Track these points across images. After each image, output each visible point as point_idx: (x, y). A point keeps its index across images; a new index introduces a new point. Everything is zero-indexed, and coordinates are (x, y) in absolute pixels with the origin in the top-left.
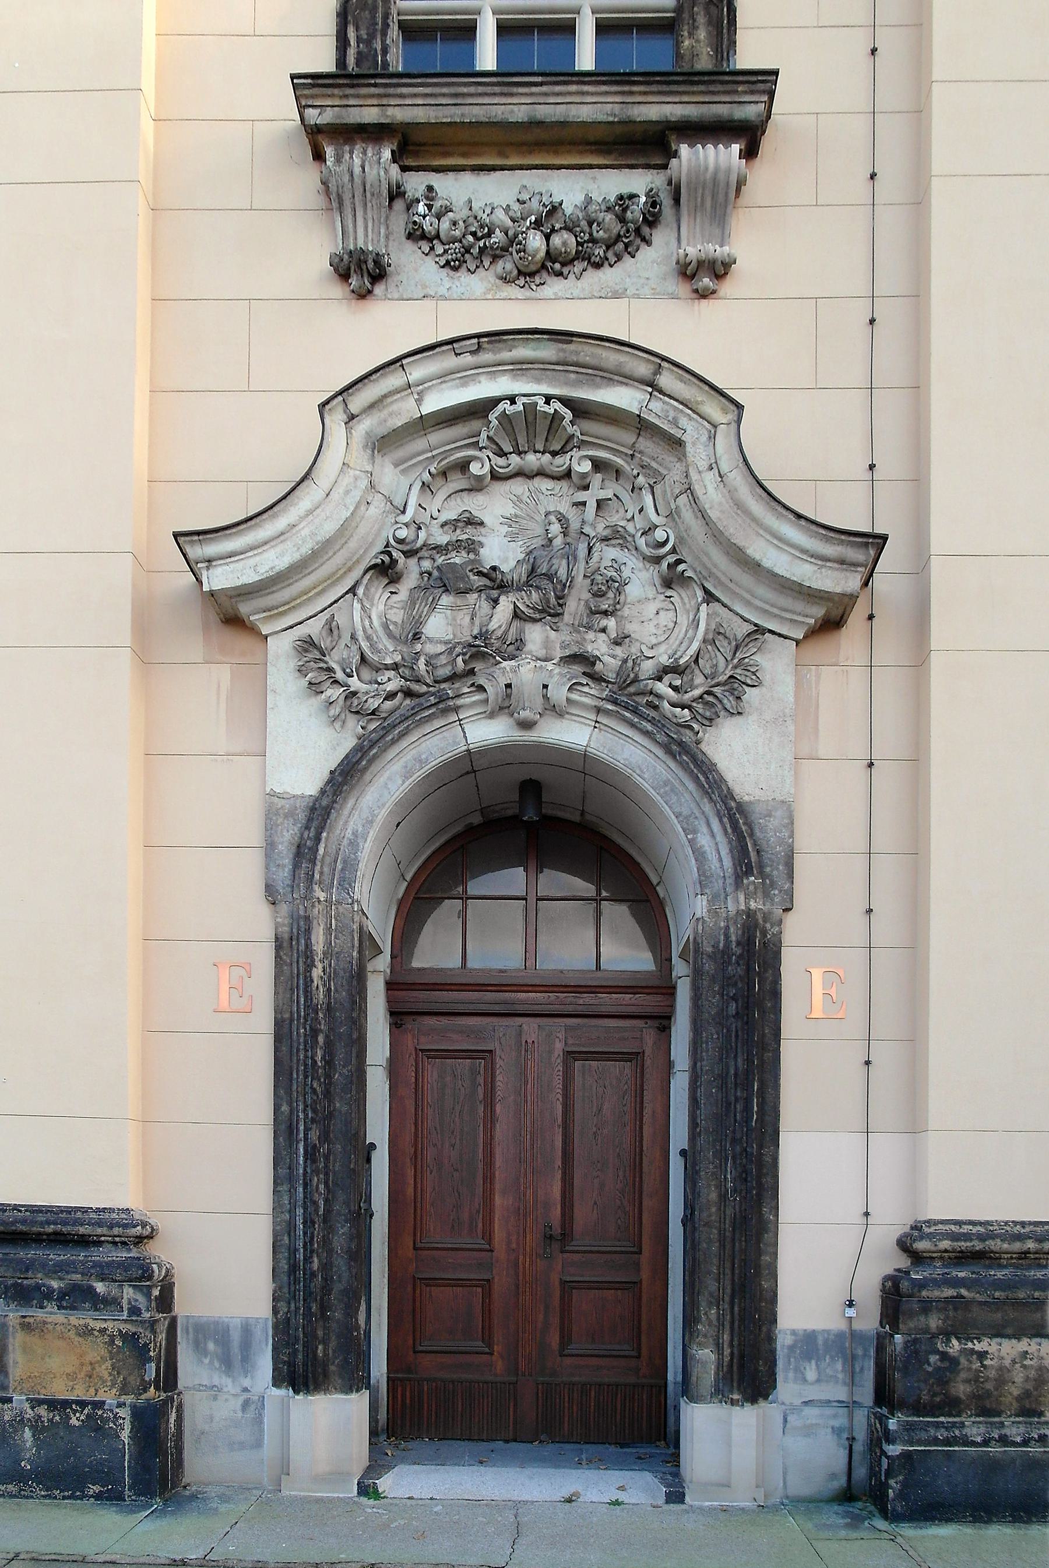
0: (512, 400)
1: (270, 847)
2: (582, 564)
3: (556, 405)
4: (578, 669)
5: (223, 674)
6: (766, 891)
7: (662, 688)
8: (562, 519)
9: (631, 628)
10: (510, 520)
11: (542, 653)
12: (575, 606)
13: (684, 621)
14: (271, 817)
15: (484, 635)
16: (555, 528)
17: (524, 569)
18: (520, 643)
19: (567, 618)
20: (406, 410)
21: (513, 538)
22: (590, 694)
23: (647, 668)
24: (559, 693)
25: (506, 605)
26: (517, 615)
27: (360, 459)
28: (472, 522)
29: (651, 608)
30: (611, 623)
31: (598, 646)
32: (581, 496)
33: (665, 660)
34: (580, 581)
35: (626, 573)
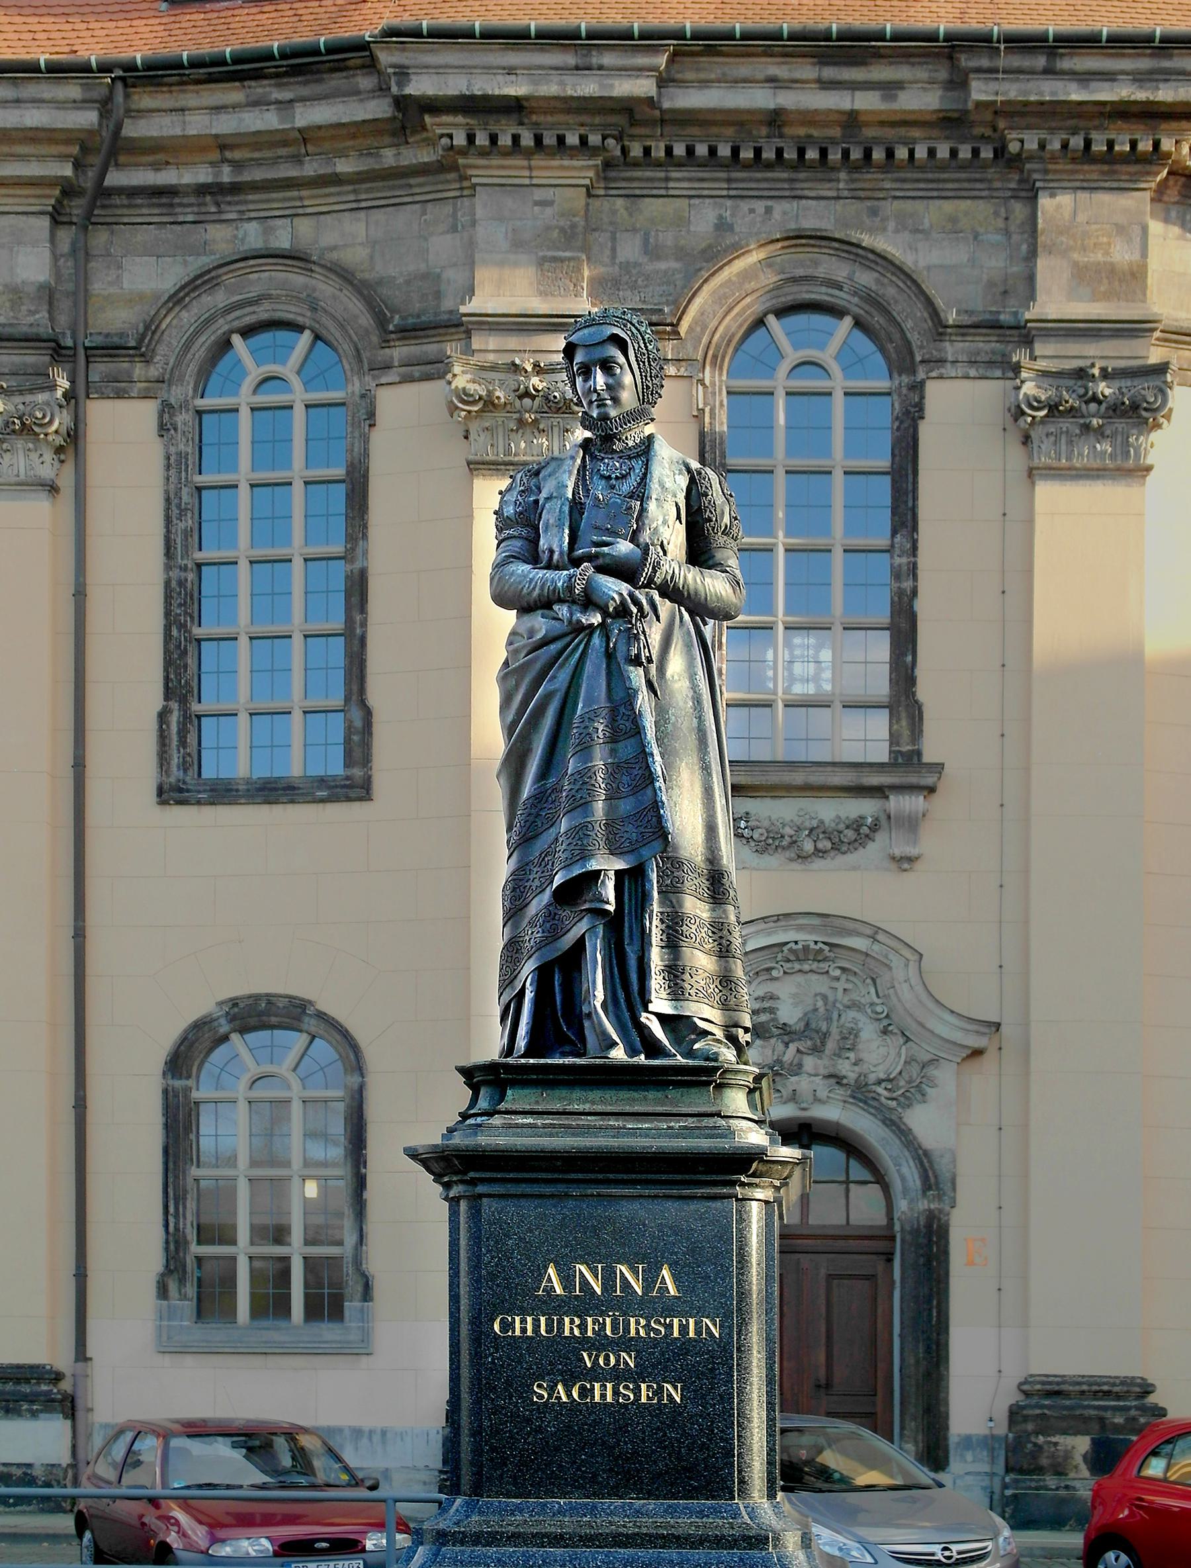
0: (796, 943)
2: (835, 1023)
3: (821, 945)
4: (833, 1081)
6: (940, 1198)
7: (880, 1090)
8: (825, 998)
9: (864, 1055)
10: (795, 996)
11: (813, 1072)
12: (831, 1045)
13: (893, 1052)
16: (820, 1004)
17: (802, 1025)
18: (800, 1066)
19: (827, 1052)
21: (796, 1005)
22: (840, 1092)
23: (872, 1078)
24: (822, 1093)
25: (792, 1047)
26: (798, 1051)
28: (772, 997)
29: (874, 1045)
30: (852, 1055)
31: (845, 1068)
32: (835, 984)
33: (882, 1076)
34: (834, 1030)
35: (861, 1025)
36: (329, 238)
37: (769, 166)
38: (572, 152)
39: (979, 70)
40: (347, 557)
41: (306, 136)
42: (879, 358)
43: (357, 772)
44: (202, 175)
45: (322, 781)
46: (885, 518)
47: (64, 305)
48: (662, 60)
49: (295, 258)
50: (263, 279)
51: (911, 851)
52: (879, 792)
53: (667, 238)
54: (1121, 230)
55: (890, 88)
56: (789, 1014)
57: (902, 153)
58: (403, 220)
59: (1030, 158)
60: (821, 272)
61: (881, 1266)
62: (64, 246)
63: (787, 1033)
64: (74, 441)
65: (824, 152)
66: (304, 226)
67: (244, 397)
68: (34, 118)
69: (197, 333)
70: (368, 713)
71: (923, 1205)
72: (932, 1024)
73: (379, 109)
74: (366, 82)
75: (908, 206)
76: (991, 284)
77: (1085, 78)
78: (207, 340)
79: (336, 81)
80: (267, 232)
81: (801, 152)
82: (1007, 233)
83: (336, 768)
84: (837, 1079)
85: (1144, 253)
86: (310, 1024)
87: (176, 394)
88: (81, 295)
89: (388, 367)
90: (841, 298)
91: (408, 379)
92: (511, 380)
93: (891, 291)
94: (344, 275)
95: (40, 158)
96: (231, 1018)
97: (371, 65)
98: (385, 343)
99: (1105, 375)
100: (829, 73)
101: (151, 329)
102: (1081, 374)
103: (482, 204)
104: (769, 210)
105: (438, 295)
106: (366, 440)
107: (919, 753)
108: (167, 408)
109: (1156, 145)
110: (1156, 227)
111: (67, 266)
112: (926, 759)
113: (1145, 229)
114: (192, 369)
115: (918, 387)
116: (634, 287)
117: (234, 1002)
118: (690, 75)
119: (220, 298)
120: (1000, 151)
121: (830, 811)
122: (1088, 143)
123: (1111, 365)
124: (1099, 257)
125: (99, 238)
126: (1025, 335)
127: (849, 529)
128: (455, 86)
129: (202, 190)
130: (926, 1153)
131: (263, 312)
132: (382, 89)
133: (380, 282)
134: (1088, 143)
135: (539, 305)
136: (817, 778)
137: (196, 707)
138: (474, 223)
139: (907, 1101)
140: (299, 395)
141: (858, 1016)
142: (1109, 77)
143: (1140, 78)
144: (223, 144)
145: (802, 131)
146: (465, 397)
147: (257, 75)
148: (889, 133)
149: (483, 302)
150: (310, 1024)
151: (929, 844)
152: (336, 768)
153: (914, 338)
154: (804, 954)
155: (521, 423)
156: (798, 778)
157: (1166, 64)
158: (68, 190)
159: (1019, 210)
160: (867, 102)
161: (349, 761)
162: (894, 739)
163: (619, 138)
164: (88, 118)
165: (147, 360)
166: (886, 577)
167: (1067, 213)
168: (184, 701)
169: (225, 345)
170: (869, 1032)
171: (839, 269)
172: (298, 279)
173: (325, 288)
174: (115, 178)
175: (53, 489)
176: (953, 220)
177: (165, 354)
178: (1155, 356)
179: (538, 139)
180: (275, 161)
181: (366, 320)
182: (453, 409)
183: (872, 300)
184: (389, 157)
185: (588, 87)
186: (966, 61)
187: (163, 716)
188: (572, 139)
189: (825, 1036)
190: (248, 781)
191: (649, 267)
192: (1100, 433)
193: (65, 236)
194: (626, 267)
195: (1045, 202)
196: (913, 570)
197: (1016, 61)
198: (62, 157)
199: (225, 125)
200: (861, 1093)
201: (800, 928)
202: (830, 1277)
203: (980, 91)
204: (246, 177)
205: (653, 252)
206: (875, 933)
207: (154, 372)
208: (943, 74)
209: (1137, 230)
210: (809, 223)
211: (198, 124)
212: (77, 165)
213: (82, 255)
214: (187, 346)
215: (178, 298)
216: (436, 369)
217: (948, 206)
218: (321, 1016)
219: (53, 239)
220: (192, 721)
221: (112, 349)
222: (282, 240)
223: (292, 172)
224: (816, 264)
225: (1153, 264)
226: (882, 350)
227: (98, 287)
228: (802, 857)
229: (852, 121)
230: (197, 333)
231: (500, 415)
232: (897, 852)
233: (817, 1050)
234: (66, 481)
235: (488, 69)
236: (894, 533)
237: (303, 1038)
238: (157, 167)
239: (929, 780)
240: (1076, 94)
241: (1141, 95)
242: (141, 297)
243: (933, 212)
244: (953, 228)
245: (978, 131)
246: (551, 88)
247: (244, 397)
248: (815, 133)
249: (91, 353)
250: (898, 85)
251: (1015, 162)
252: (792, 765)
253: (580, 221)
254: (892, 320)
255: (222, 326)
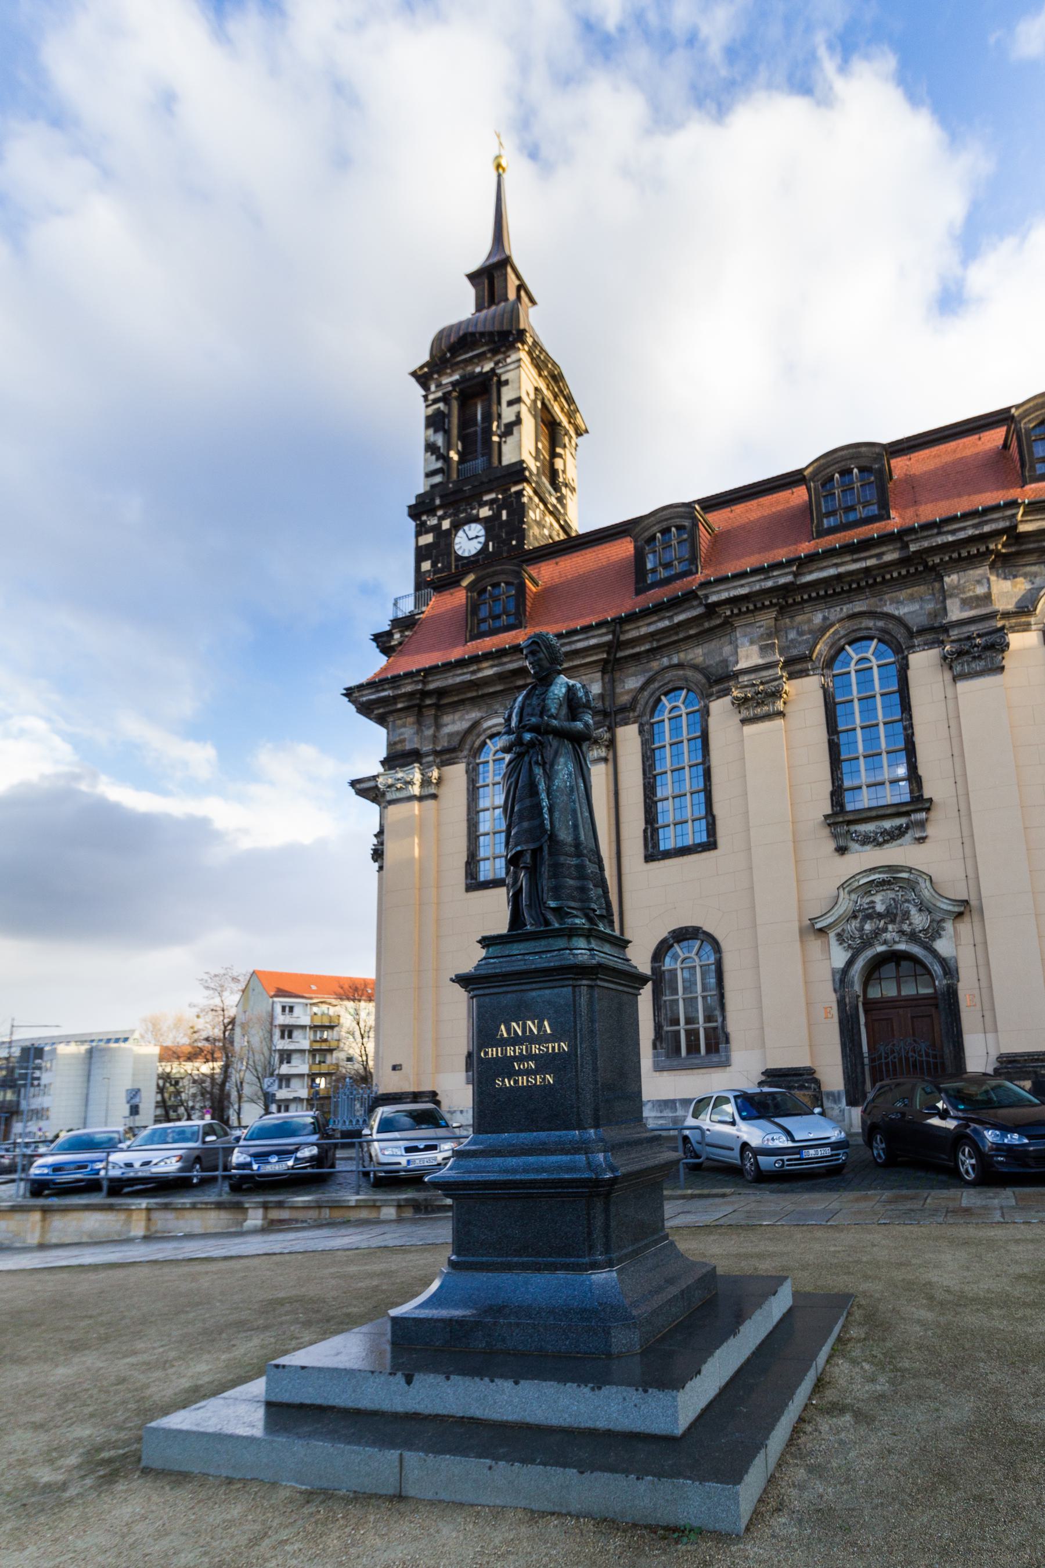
1: (834, 980)
5: (819, 942)
6: (952, 978)
12: (898, 919)
14: (834, 972)
15: (878, 928)
20: (856, 884)
22: (904, 938)
24: (897, 939)
25: (882, 922)
27: (847, 896)
28: (873, 902)
31: (905, 927)
36: (690, 656)
37: (839, 594)
38: (768, 607)
39: (912, 540)
40: (703, 763)
41: (680, 624)
42: (889, 651)
43: (712, 839)
44: (647, 647)
45: (700, 845)
46: (898, 709)
47: (607, 698)
48: (794, 568)
49: (680, 666)
50: (669, 675)
51: (924, 835)
52: (907, 814)
53: (806, 628)
54: (979, 582)
55: (879, 556)
56: (880, 908)
57: (888, 577)
58: (713, 645)
59: (938, 565)
60: (863, 625)
61: (933, 1009)
62: (607, 680)
63: (880, 916)
64: (612, 744)
65: (858, 584)
66: (682, 655)
67: (666, 715)
68: (593, 642)
69: (650, 697)
70: (714, 817)
71: (945, 982)
72: (939, 904)
73: (700, 610)
74: (695, 603)
75: (894, 594)
76: (930, 614)
77: (953, 532)
78: (652, 700)
79: (686, 605)
80: (670, 659)
81: (850, 586)
82: (934, 594)
83: (704, 839)
84: (902, 932)
85: (989, 588)
86: (701, 936)
87: (645, 719)
88: (613, 695)
89: (711, 695)
90: (873, 633)
91: (719, 697)
92: (753, 689)
93: (891, 626)
94: (695, 667)
95: (596, 654)
96: (673, 937)
97: (697, 597)
98: (711, 687)
99: (979, 636)
100: (855, 556)
101: (634, 701)
102: (969, 638)
103: (738, 634)
104: (841, 609)
105: (727, 667)
106: (707, 721)
107: (922, 796)
108: (641, 726)
109: (987, 548)
110: (993, 578)
111: (608, 686)
112: (926, 796)
113: (988, 580)
114: (648, 710)
115: (906, 658)
116: (795, 647)
117: (674, 931)
118: (805, 570)
119: (656, 685)
120: (926, 566)
121: (887, 824)
122: (959, 554)
123: (981, 632)
124: (971, 594)
125: (617, 675)
126: (945, 629)
127: (884, 716)
128: (724, 595)
129: (648, 651)
130: (944, 959)
131: (670, 686)
132: (701, 603)
133: (708, 667)
134: (959, 554)
135: (760, 661)
136: (881, 812)
137: (656, 826)
138: (737, 639)
139: (933, 938)
140: (683, 710)
141: (911, 906)
142: (964, 529)
143: (975, 526)
144: (652, 635)
145: (849, 579)
146: (736, 698)
147: (661, 610)
148: (882, 571)
149: (742, 665)
150: (701, 936)
151: (931, 830)
152: (704, 839)
153: (902, 640)
154: (883, 883)
155: (758, 703)
156: (874, 813)
157: (985, 518)
158: (605, 661)
159: (937, 585)
160: (871, 562)
161: (708, 836)
162: (911, 792)
163: (783, 598)
164: (609, 637)
165: (634, 710)
166: (901, 730)
167: (956, 582)
168: (652, 824)
169: (659, 700)
170: (913, 911)
171: (870, 623)
172: (681, 672)
173: (689, 673)
174: (620, 654)
175: (605, 760)
176: (912, 595)
177: (639, 708)
178: (999, 624)
179: (755, 606)
180: (670, 636)
181: (704, 681)
182: (733, 704)
183: (883, 631)
184: (707, 625)
185: (770, 584)
186: (906, 539)
187: (645, 831)
188: (767, 603)
189: (896, 915)
190: (675, 849)
191: (800, 639)
192: (979, 657)
193: (607, 678)
194: (792, 641)
195: (947, 579)
196: (911, 726)
197: (925, 534)
198: (603, 652)
199: (652, 628)
200: (913, 937)
201: (880, 873)
202: (913, 1017)
203: (913, 548)
204: (661, 643)
205: (801, 633)
206: (910, 870)
207: (636, 714)
208: (899, 545)
209: (985, 581)
210: (857, 609)
211: (644, 631)
212: (608, 653)
213: (613, 681)
214: (647, 703)
215: (642, 688)
216: (726, 692)
217: (909, 591)
218: (705, 933)
219: (603, 679)
220: (655, 831)
221: (623, 709)
222: (675, 661)
223: (675, 638)
224: (861, 623)
225: (995, 591)
226: (890, 647)
227: (618, 690)
228: (880, 844)
229: (867, 570)
230: (650, 697)
231: (750, 703)
232: (917, 836)
233: (893, 921)
234: (610, 757)
235: (735, 588)
236: (902, 713)
237: (699, 942)
238: (633, 648)
239: (927, 805)
240: (951, 538)
241: (977, 532)
242: (631, 690)
243: (903, 595)
244: (912, 598)
245: (916, 561)
246: (757, 587)
247: (666, 715)
248: (854, 578)
249: (616, 713)
250: (883, 554)
251: (934, 568)
252: (870, 809)
253: (773, 630)
254: (892, 636)
255: (657, 694)
